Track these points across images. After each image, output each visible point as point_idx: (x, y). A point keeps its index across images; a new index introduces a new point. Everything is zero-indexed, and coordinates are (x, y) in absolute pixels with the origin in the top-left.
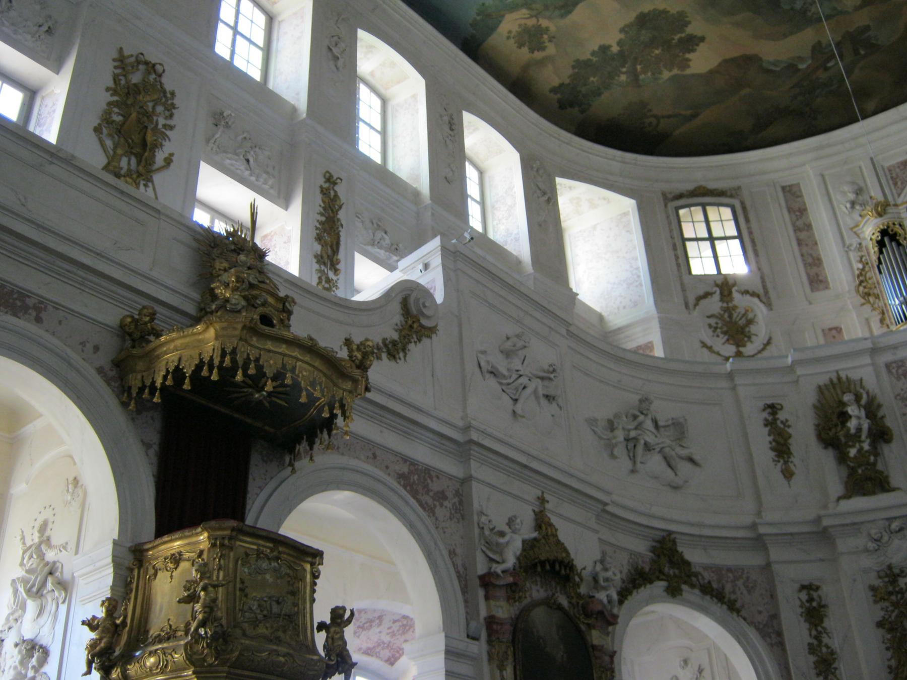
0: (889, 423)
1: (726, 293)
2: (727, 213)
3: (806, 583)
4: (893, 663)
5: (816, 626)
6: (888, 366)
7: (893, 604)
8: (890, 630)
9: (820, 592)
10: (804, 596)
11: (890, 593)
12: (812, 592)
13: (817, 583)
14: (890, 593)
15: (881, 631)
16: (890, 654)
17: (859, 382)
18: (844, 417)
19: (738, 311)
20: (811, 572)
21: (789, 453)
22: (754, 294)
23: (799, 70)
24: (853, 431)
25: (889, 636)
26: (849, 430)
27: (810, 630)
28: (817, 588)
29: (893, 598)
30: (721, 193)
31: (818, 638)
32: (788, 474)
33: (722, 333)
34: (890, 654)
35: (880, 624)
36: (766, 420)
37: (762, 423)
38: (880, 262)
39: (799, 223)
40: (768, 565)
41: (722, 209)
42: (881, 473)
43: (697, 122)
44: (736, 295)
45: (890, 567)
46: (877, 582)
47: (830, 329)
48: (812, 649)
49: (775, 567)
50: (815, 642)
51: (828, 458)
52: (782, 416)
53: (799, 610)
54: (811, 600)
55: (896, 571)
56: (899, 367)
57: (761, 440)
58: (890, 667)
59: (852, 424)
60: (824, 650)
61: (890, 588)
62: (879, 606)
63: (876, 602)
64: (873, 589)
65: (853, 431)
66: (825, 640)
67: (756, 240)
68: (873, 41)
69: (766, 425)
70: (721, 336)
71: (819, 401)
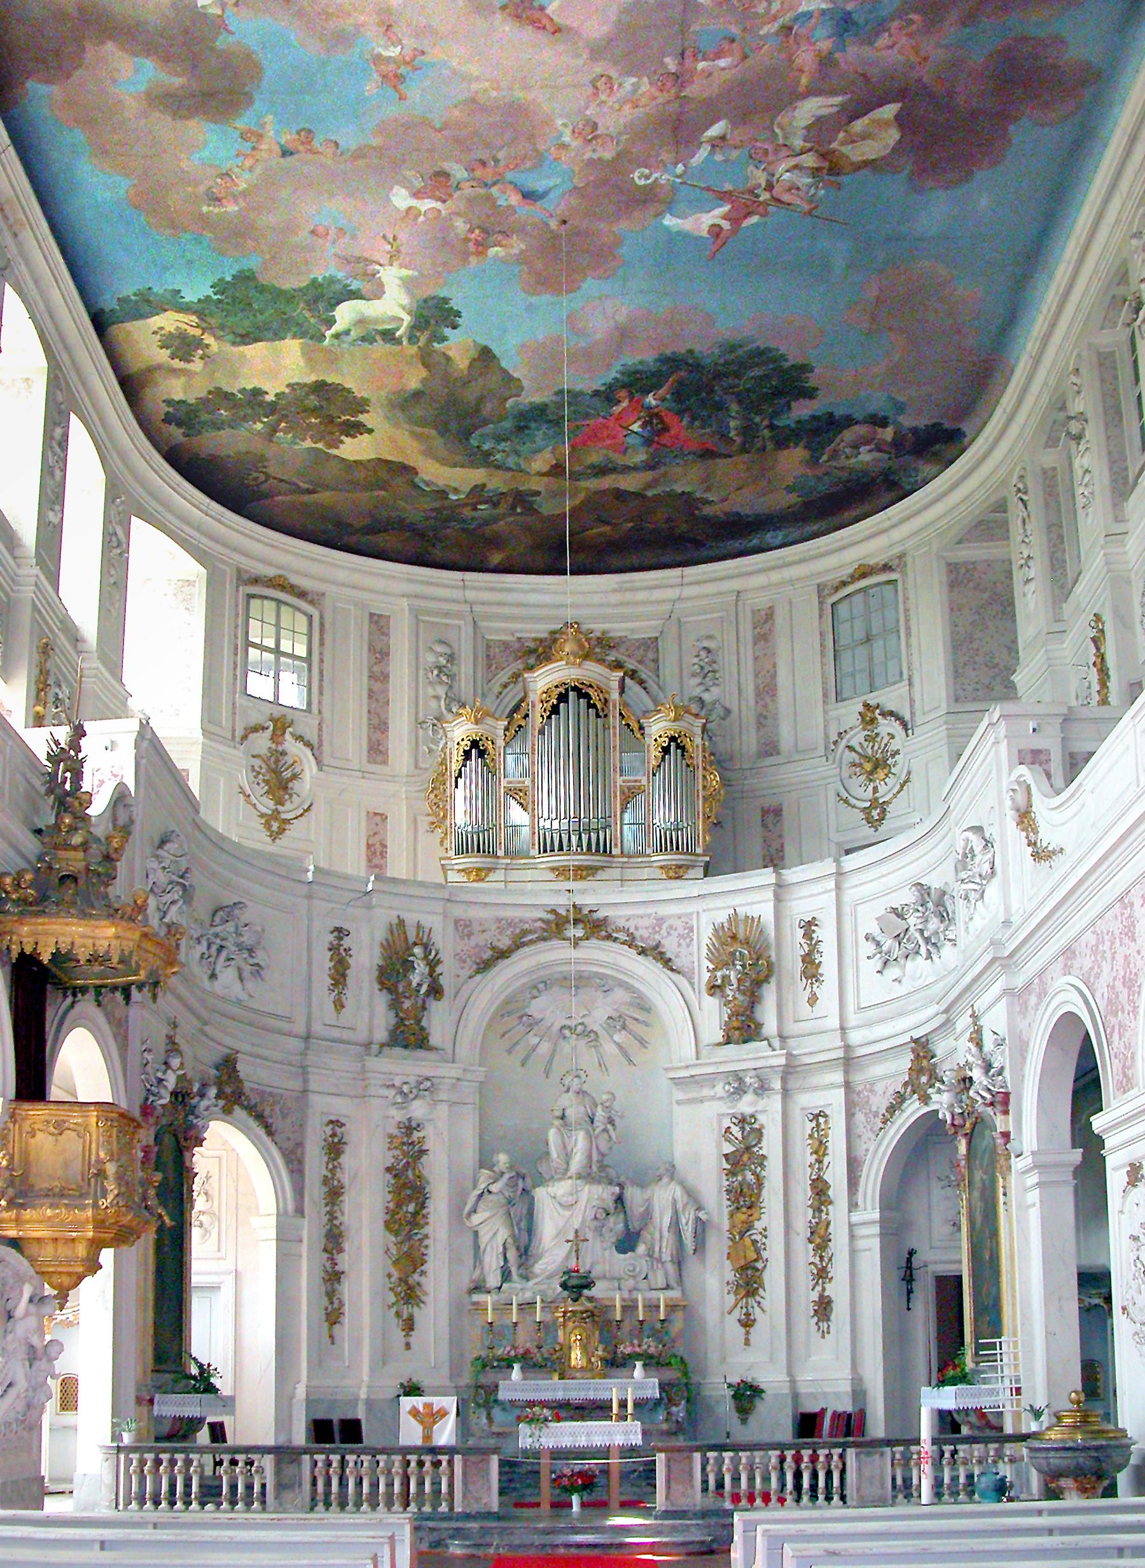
0: (443, 981)
1: (279, 733)
2: (302, 623)
3: (334, 1118)
4: (392, 1205)
5: (335, 1160)
6: (457, 922)
7: (403, 1152)
8: (395, 1176)
9: (343, 1129)
10: (328, 1130)
11: (404, 1144)
12: (337, 1128)
13: (343, 1120)
14: (404, 1144)
15: (388, 1176)
16: (390, 1197)
17: (427, 930)
18: (409, 966)
19: (286, 758)
20: (340, 1107)
21: (345, 985)
22: (308, 744)
23: (447, 498)
24: (414, 984)
25: (393, 1181)
26: (410, 983)
27: (328, 1163)
28: (343, 1125)
29: (405, 1148)
30: (302, 594)
31: (333, 1171)
32: (339, 1005)
33: (264, 781)
34: (390, 1197)
35: (388, 1169)
36: (331, 943)
37: (327, 945)
38: (460, 775)
39: (377, 669)
40: (305, 1091)
41: (299, 615)
42: (422, 1029)
43: (307, 498)
44: (287, 736)
45: (410, 1120)
46: (396, 1132)
47: (376, 814)
48: (326, 1181)
49: (314, 1098)
50: (330, 1175)
51: (382, 1000)
52: (346, 942)
53: (323, 1143)
54: (334, 1135)
55: (414, 1124)
56: (466, 926)
57: (324, 962)
58: (387, 1208)
59: (415, 979)
60: (336, 1183)
61: (405, 1140)
62: (391, 1153)
63: (389, 1149)
64: (391, 1136)
65: (414, 984)
66: (338, 1175)
67: (325, 673)
68: (535, 506)
69: (330, 950)
70: (263, 785)
71: (387, 940)
